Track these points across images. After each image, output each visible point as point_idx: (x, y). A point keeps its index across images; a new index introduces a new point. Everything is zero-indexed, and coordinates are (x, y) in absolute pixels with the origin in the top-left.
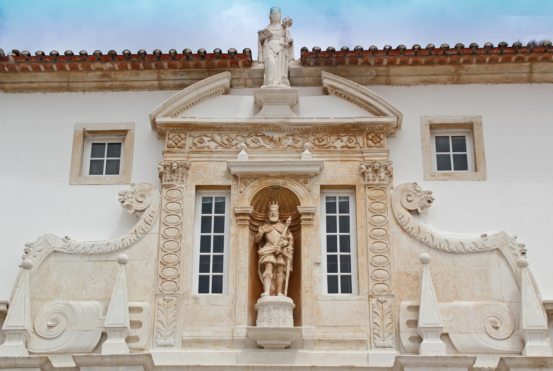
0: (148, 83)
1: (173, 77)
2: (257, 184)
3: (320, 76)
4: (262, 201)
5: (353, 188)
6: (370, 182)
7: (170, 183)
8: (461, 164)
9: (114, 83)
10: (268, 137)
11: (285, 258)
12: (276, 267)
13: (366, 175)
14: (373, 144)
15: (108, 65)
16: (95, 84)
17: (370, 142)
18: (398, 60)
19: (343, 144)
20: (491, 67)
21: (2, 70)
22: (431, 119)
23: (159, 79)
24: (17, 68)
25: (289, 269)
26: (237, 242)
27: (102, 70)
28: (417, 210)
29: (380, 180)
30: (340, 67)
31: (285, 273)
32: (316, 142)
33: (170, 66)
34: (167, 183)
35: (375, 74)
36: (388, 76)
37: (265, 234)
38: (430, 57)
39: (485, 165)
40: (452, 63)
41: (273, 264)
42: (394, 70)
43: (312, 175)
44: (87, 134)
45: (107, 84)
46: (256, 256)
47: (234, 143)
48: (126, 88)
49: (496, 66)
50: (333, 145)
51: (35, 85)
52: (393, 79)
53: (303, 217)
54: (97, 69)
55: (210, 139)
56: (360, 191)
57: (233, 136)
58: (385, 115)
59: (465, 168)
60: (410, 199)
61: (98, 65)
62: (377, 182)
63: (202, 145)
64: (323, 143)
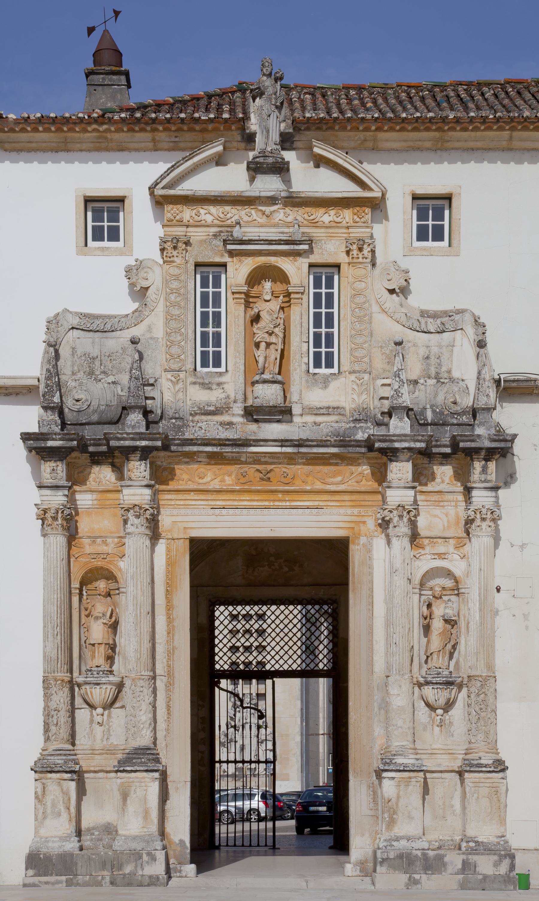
0: (143, 145)
1: (167, 139)
2: (251, 262)
3: (311, 142)
4: (256, 278)
5: (338, 266)
6: (355, 260)
7: (172, 259)
8: (438, 236)
9: (110, 144)
10: (261, 210)
11: (276, 335)
12: (268, 345)
13: (351, 253)
14: (358, 220)
15: (105, 127)
16: (91, 145)
17: (355, 217)
18: (386, 128)
19: (331, 219)
20: (473, 134)
21: (1, 130)
22: (413, 188)
23: (154, 140)
24: (17, 129)
25: (280, 347)
26: (233, 314)
27: (98, 131)
28: (394, 289)
29: (363, 258)
30: (329, 133)
31: (277, 350)
32: (306, 216)
33: (166, 129)
34: (169, 259)
35: (363, 138)
36: (375, 140)
37: (259, 311)
38: (416, 125)
39: (460, 240)
40: (438, 129)
41: (266, 342)
42: (381, 135)
43: (302, 252)
44: (88, 200)
45: (103, 145)
46: (249, 335)
47: (229, 216)
48: (121, 149)
49: (479, 134)
50: (321, 219)
51: (34, 145)
52: (381, 145)
53: (292, 296)
54: (94, 130)
55: (206, 211)
56: (344, 268)
57: (228, 208)
58: (370, 189)
59: (442, 239)
60: (390, 277)
61: (95, 126)
62: (360, 260)
63: (199, 219)
64: (312, 217)
